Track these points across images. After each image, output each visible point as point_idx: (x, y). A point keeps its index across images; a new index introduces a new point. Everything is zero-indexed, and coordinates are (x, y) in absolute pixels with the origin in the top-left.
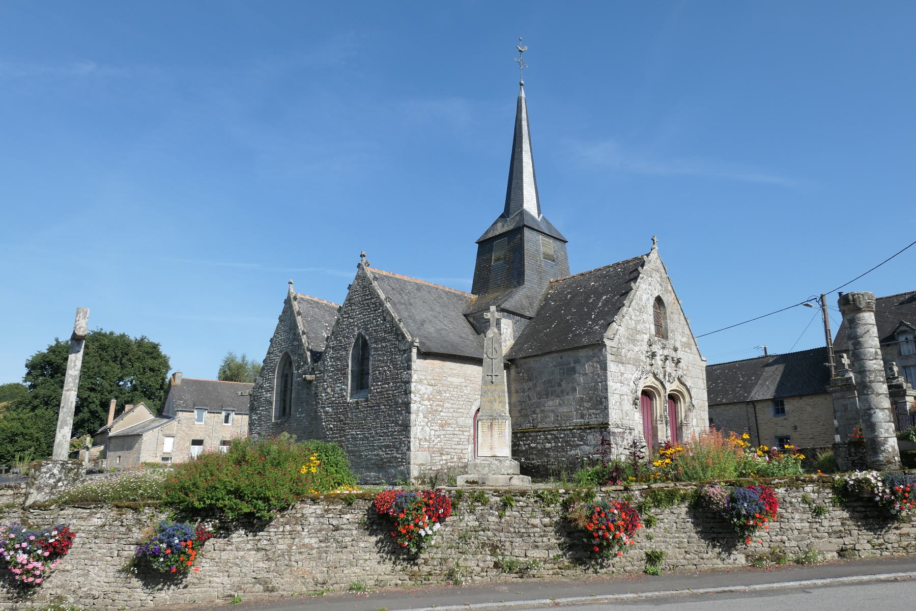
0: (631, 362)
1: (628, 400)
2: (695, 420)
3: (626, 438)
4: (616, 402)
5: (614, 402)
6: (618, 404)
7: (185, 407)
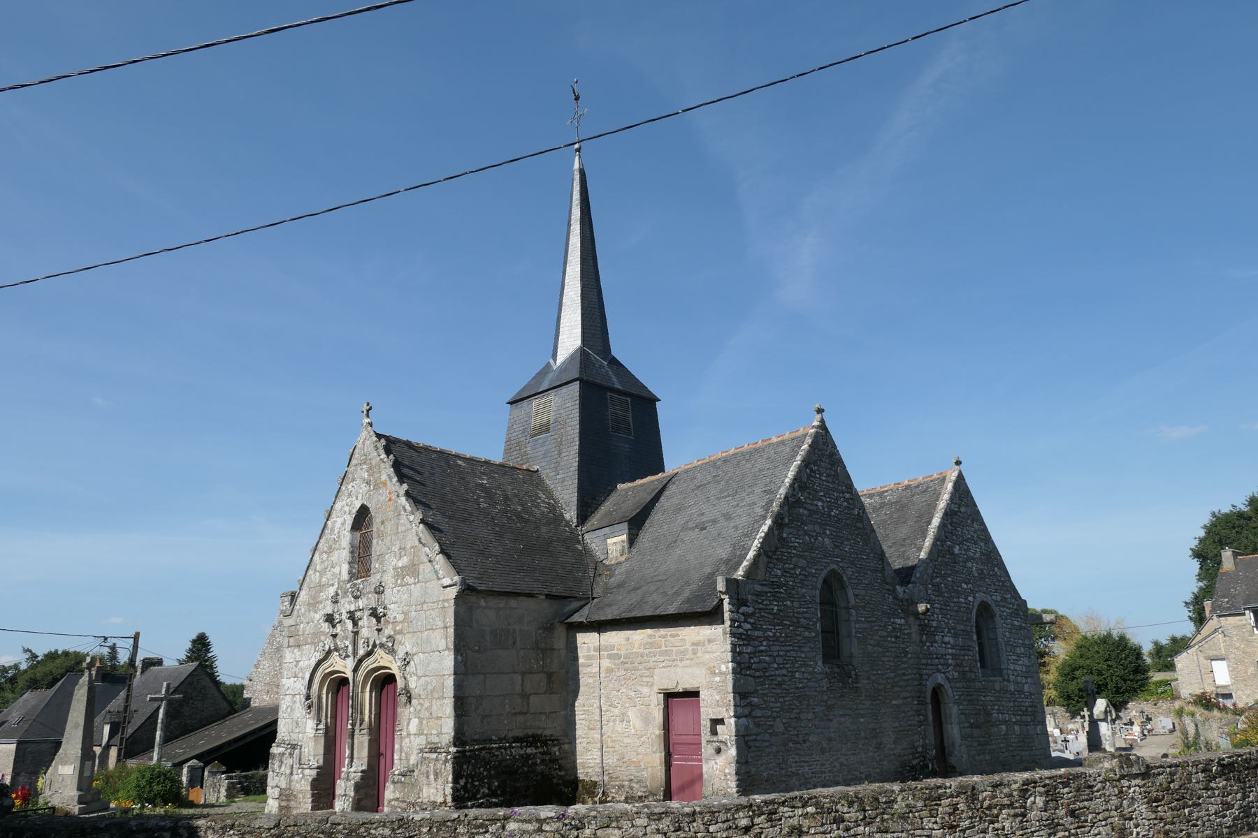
0: (309, 641)
2: (415, 722)
3: (285, 762)
4: (287, 708)
5: (285, 707)
6: (289, 710)
7: (1228, 609)
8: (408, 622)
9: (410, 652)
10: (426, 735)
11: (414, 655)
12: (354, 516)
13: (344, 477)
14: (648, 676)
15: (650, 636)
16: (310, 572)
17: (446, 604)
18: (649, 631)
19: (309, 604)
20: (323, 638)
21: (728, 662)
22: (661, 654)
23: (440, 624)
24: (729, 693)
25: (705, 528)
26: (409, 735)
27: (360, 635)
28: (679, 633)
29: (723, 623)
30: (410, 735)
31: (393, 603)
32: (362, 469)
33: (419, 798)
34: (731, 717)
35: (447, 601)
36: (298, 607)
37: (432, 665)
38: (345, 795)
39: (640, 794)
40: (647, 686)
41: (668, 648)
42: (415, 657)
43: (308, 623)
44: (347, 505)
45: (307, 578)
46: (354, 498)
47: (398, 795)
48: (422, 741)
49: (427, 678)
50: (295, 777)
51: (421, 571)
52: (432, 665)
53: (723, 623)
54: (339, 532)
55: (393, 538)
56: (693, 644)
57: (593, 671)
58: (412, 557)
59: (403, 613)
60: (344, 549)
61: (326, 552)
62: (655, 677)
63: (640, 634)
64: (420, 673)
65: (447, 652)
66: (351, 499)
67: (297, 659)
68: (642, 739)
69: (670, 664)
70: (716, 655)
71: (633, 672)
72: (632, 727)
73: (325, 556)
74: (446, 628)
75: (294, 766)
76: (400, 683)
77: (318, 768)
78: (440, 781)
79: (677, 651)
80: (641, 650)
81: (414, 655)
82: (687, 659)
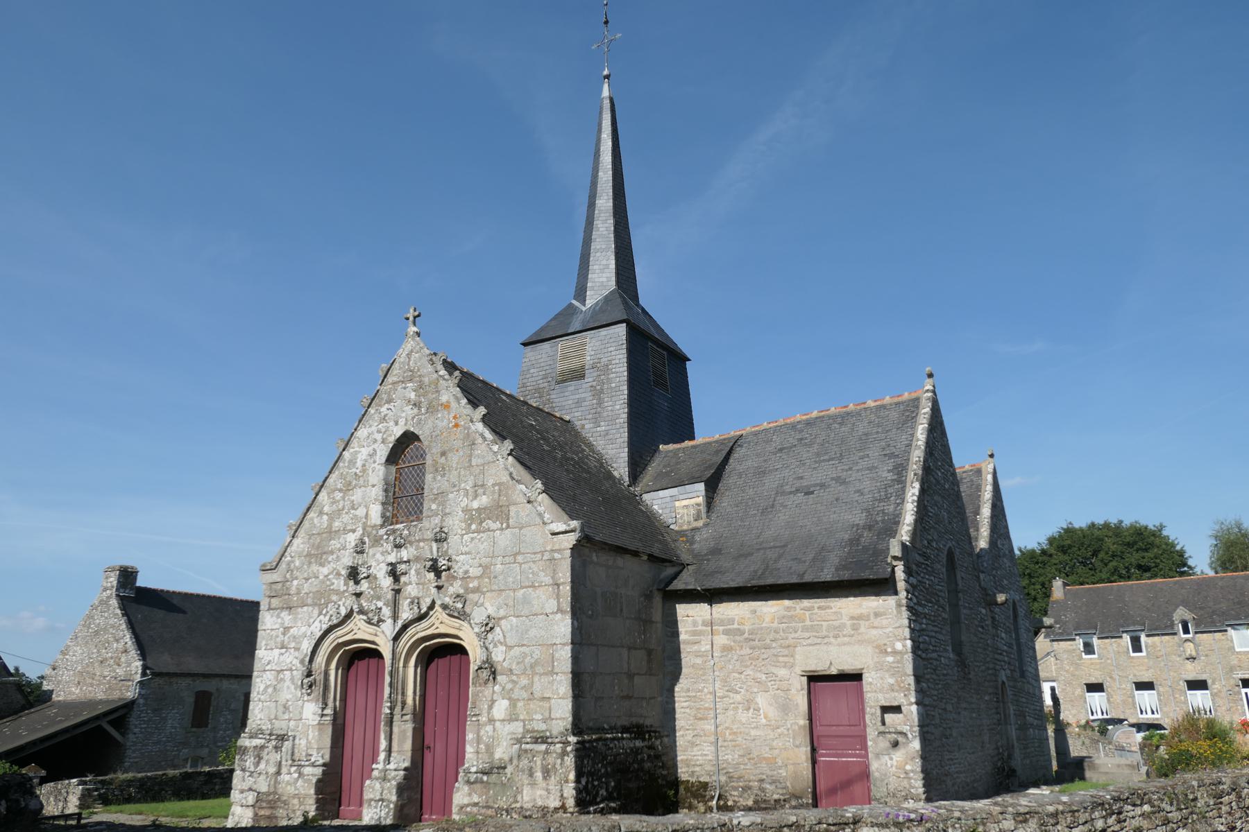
0: (310, 601)
1: (292, 679)
3: (266, 757)
4: (267, 687)
5: (262, 687)
6: (270, 690)
7: (1061, 634)
8: (489, 578)
9: (493, 615)
10: (524, 721)
11: (500, 619)
12: (391, 445)
13: (374, 397)
14: (787, 656)
15: (788, 609)
16: (311, 515)
17: (557, 556)
18: (787, 602)
19: (309, 555)
20: (334, 598)
21: (905, 639)
22: (805, 629)
23: (548, 580)
24: (909, 675)
25: (812, 493)
26: (491, 721)
27: (403, 594)
28: (832, 605)
29: (896, 593)
30: (494, 721)
31: (462, 554)
32: (405, 388)
33: (517, 802)
34: (911, 704)
35: (559, 551)
36: (289, 558)
37: (533, 632)
38: (382, 800)
39: (776, 797)
40: (785, 667)
41: (815, 623)
42: (503, 622)
43: (307, 579)
44: (379, 432)
45: (306, 522)
46: (392, 423)
47: (476, 799)
48: (518, 728)
49: (522, 649)
50: (285, 777)
51: (512, 514)
52: (533, 632)
53: (896, 593)
54: (364, 465)
55: (463, 473)
56: (852, 618)
57: (703, 650)
58: (496, 496)
59: (480, 565)
60: (373, 486)
61: (340, 490)
62: (797, 657)
63: (772, 606)
64: (510, 642)
65: (559, 616)
66: (385, 424)
67: (286, 625)
68: (779, 730)
69: (819, 641)
70: (887, 631)
71: (763, 651)
72: (762, 716)
73: (338, 495)
74: (558, 585)
75: (284, 763)
76: (476, 654)
77: (324, 765)
78: (553, 780)
79: (828, 625)
80: (775, 625)
81: (500, 619)
82: (844, 636)
